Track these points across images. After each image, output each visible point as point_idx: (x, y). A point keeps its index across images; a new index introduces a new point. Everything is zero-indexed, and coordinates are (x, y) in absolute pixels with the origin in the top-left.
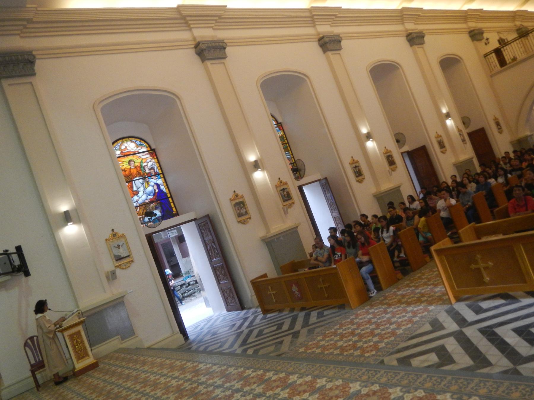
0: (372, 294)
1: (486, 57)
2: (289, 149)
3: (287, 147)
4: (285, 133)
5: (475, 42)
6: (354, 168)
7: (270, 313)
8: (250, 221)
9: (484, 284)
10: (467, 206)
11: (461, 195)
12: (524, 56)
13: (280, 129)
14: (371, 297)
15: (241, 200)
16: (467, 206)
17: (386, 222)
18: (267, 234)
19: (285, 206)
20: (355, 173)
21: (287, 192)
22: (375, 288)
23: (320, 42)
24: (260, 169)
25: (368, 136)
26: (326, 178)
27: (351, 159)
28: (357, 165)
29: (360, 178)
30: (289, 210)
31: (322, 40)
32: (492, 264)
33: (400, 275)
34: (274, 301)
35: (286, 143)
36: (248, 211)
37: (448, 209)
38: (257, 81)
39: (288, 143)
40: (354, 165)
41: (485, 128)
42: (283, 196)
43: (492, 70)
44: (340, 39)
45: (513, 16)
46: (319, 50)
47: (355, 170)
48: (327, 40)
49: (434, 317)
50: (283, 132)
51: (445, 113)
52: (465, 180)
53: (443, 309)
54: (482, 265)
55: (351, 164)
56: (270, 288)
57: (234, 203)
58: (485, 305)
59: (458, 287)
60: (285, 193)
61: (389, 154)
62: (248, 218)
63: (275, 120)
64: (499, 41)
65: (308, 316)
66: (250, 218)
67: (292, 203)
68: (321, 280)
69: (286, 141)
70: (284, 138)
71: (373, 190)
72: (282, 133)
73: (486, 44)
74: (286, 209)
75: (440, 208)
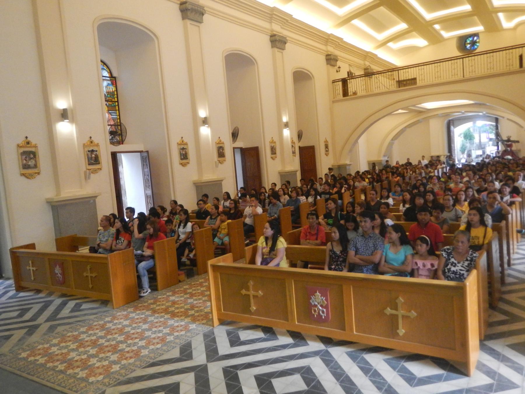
0: (144, 293)
2: (117, 109)
3: (115, 106)
4: (117, 90)
5: (329, 66)
6: (181, 149)
7: (24, 292)
8: (38, 177)
9: (250, 312)
10: (273, 218)
11: (271, 205)
13: (112, 84)
14: (141, 297)
15: (33, 150)
16: (273, 218)
17: (186, 216)
18: (57, 195)
19: (89, 169)
20: (181, 154)
21: (95, 155)
22: (150, 287)
23: (182, 6)
24: (68, 121)
25: (205, 121)
26: (147, 152)
27: (180, 138)
28: (185, 147)
29: (185, 161)
30: (92, 175)
31: (184, 5)
32: (262, 294)
33: (183, 277)
34: (33, 278)
35: (115, 102)
36: (38, 165)
37: (253, 217)
38: (95, 19)
39: (118, 101)
40: (182, 146)
41: (316, 147)
42: (90, 159)
43: (335, 97)
44: (204, 12)
45: (366, 56)
46: (179, 14)
47: (182, 152)
48: (189, 7)
49: (189, 339)
50: (115, 88)
51: (284, 122)
53: (203, 331)
54: (252, 293)
55: (179, 144)
56: (30, 262)
57: (22, 150)
58: (244, 335)
59: (224, 310)
60: (93, 156)
61: (221, 145)
62: (36, 173)
63: (109, 72)
64: (348, 73)
65: (64, 304)
66: (39, 173)
67: (98, 169)
68: (88, 267)
69: (116, 99)
70: (114, 95)
71: (195, 178)
72: (114, 89)
73: (337, 72)
74: (88, 174)
75: (246, 214)
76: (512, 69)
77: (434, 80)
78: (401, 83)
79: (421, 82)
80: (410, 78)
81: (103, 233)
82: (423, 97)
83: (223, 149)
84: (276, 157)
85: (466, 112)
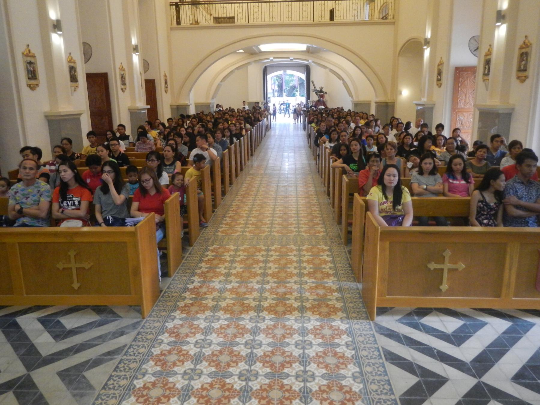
1: (172, 6)
6: (28, 63)
12: (245, 22)
20: (28, 71)
27: (25, 47)
28: (33, 61)
40: (29, 59)
43: (173, 23)
47: (29, 68)
52: (183, 131)
71: (46, 108)
76: (322, 21)
77: (285, 19)
78: (218, 20)
79: (239, 21)
80: (228, 16)
81: (22, 190)
82: (261, 38)
83: (75, 71)
84: (126, 89)
85: (294, 58)
